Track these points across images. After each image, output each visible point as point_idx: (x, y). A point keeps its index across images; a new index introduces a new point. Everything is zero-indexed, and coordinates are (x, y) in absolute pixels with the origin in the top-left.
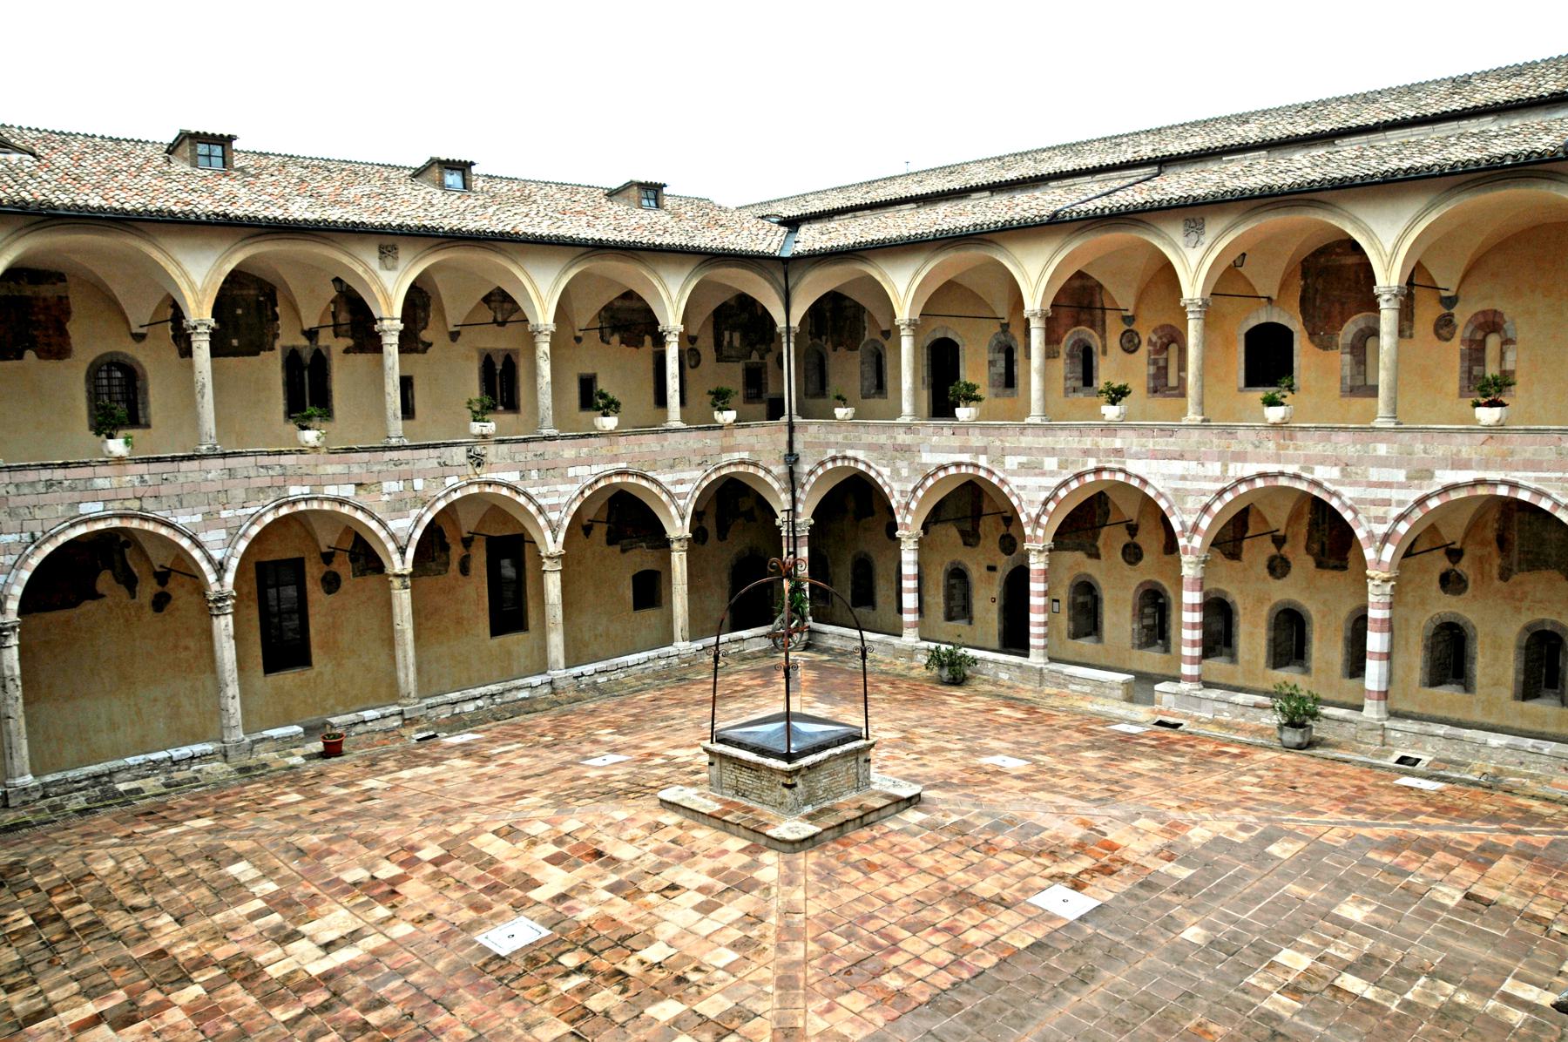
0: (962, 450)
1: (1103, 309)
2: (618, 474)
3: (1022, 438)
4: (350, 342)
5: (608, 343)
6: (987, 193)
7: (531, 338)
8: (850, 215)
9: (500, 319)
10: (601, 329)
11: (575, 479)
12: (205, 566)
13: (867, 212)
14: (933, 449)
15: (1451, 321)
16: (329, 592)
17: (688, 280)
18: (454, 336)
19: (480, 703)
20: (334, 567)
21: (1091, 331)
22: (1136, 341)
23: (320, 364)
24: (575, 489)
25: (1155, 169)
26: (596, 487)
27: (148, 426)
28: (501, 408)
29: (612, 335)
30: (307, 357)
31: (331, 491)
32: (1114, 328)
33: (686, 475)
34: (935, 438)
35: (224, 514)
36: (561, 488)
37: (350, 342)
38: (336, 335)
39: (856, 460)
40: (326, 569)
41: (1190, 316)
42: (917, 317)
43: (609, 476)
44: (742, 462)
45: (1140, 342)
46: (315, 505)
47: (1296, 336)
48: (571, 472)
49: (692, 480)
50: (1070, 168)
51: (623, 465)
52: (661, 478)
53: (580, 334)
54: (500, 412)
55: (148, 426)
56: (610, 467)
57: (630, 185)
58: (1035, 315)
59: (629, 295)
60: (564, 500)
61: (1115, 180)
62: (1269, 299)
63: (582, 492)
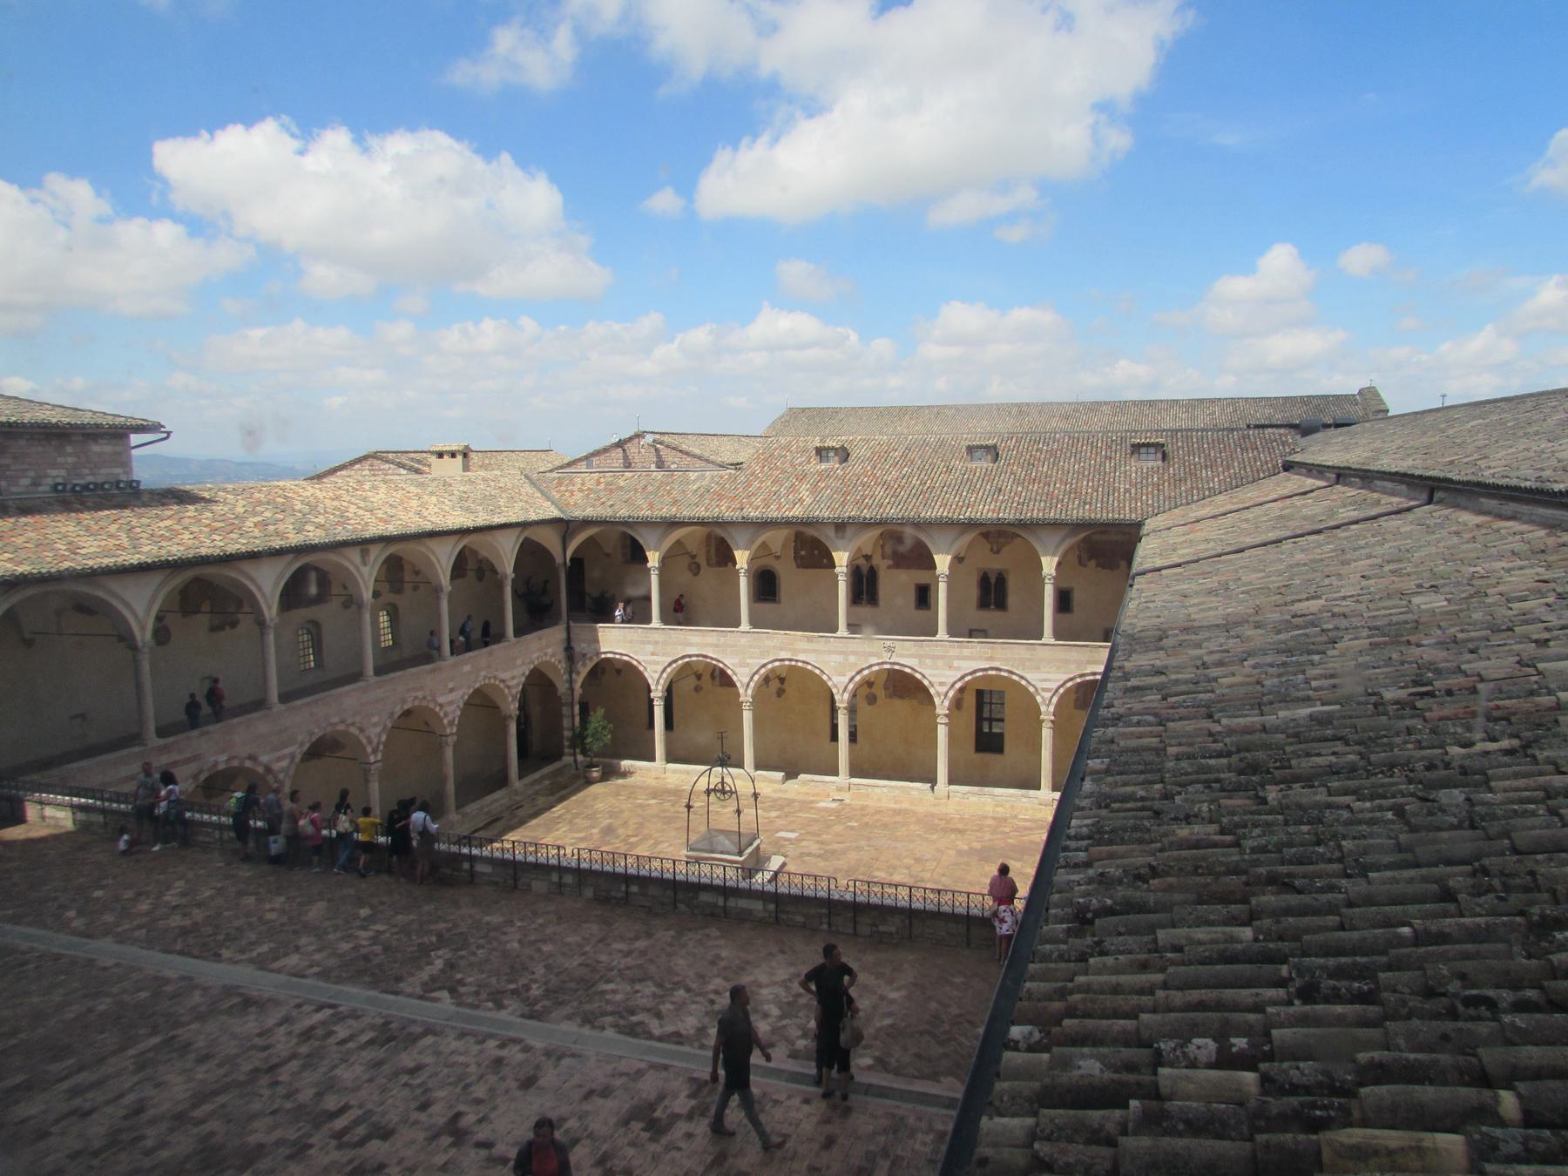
4: (891, 562)
5: (1085, 566)
9: (995, 549)
11: (958, 668)
12: (738, 685)
16: (869, 704)
17: (1063, 540)
19: (885, 790)
20: (873, 690)
23: (873, 573)
24: (959, 675)
26: (974, 676)
27: (779, 603)
28: (992, 607)
29: (1090, 560)
30: (865, 570)
31: (801, 657)
35: (748, 661)
36: (948, 673)
37: (891, 562)
38: (883, 558)
40: (868, 690)
46: (793, 663)
48: (956, 664)
49: (1058, 680)
51: (997, 664)
52: (1028, 676)
55: (779, 603)
60: (952, 681)
63: (963, 677)
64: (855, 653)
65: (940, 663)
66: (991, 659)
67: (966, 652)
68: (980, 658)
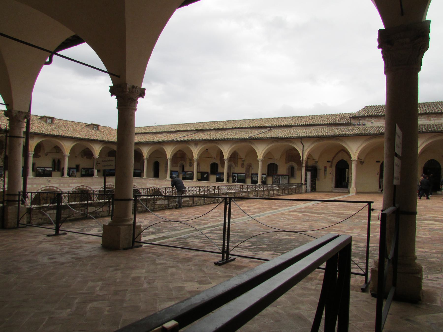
0: (155, 184)
1: (186, 158)
2: (82, 186)
3: (166, 182)
5: (83, 158)
6: (166, 133)
7: (64, 157)
8: (140, 134)
10: (82, 155)
11: (71, 187)
13: (143, 134)
14: (150, 184)
15: (244, 164)
18: (46, 155)
21: (184, 162)
22: (192, 164)
25: (196, 132)
28: (56, 171)
32: (188, 162)
33: (97, 187)
34: (150, 182)
39: (135, 185)
41: (195, 161)
42: (148, 157)
43: (79, 186)
44: (110, 185)
45: (192, 164)
47: (219, 166)
48: (71, 185)
50: (181, 130)
51: (83, 184)
52: (92, 187)
53: (76, 156)
54: (56, 172)
56: (80, 185)
57: (91, 124)
58: (169, 159)
59: (88, 148)
61: (184, 134)
62: (215, 158)
64: (35, 184)
65: (66, 185)
66: (81, 183)
67: (74, 181)
68: (78, 183)
